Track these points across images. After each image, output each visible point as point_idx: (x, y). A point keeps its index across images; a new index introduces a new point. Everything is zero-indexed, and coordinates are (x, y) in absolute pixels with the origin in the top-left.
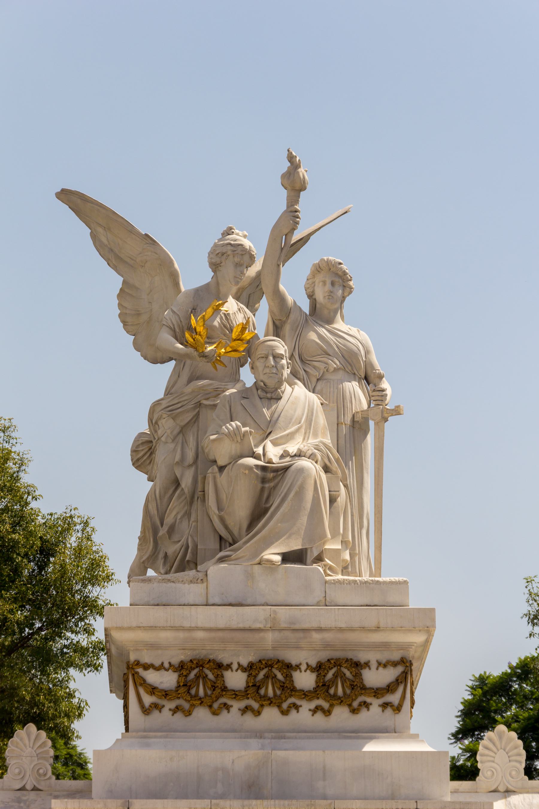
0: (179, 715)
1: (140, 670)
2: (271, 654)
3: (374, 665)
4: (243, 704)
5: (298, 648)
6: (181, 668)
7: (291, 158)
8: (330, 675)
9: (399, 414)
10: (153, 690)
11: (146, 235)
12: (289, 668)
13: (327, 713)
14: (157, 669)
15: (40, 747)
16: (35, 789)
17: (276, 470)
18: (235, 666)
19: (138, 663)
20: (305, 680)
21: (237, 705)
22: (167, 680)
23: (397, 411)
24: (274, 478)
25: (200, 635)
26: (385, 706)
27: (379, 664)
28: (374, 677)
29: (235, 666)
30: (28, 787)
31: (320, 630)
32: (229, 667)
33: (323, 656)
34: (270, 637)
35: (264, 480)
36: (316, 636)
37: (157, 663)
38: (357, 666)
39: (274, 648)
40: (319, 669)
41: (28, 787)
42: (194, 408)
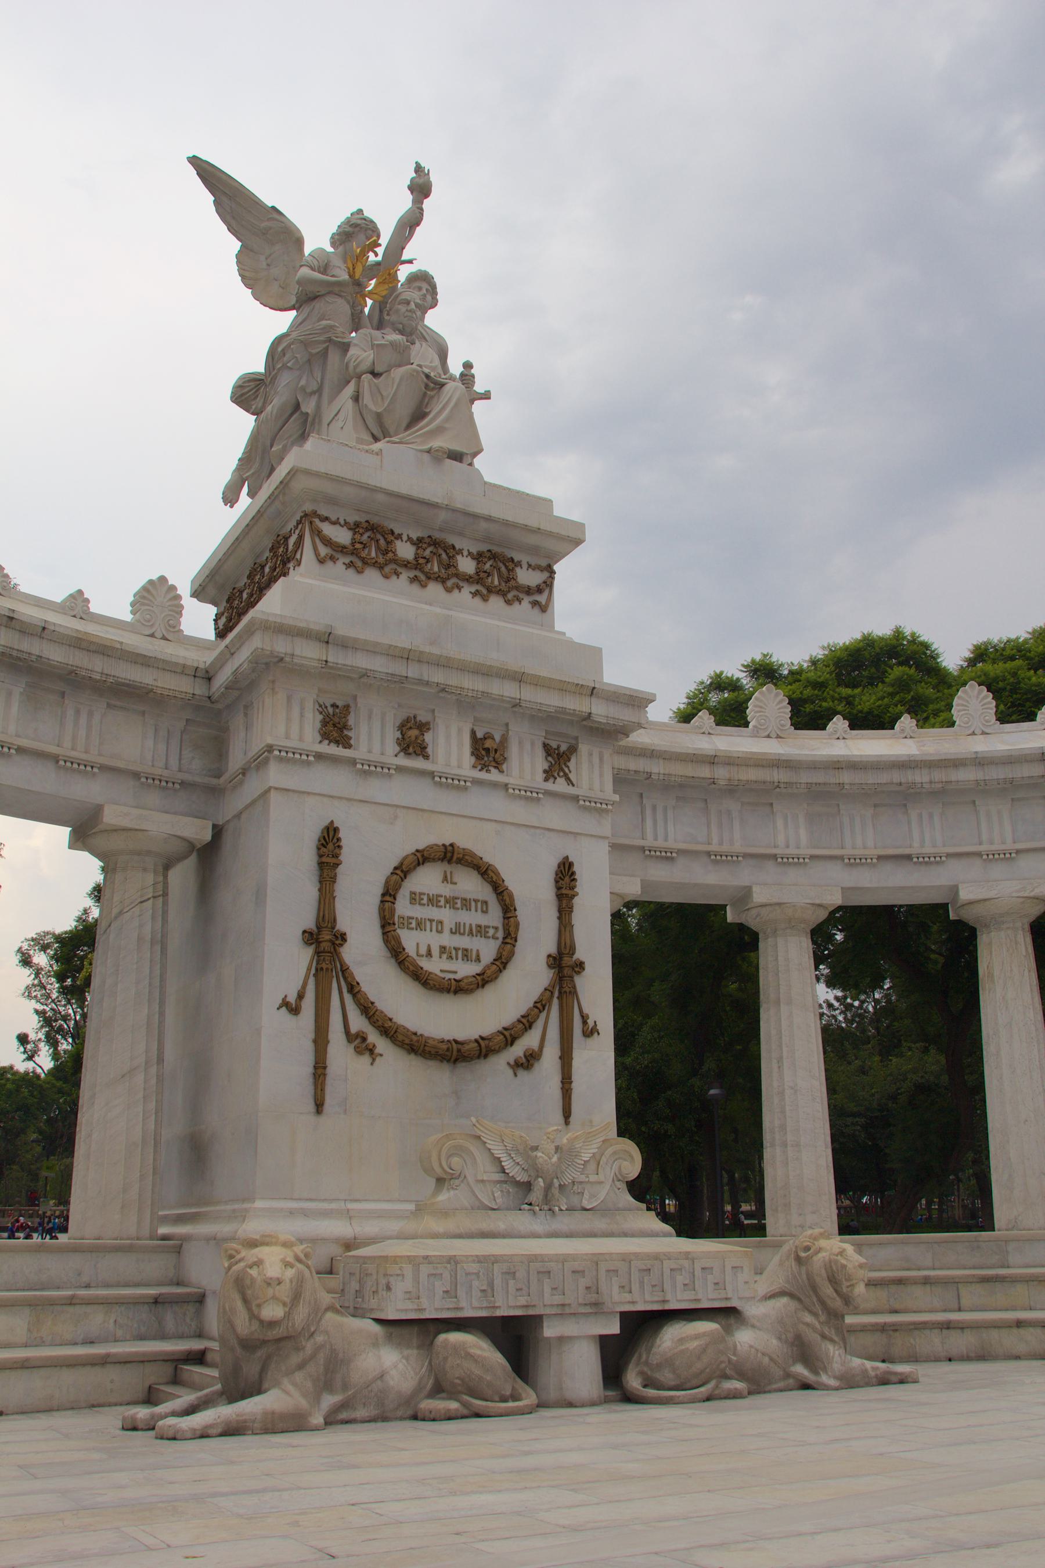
0: (351, 571)
1: (317, 521)
2: (437, 535)
3: (525, 566)
4: (412, 574)
5: (461, 534)
6: (355, 527)
7: (419, 169)
8: (487, 566)
9: (489, 398)
10: (328, 542)
11: (273, 208)
12: (452, 551)
13: (485, 599)
14: (334, 523)
15: (170, 599)
16: (164, 638)
17: (436, 383)
18: (405, 538)
19: (315, 514)
20: (466, 565)
21: (405, 575)
22: (343, 536)
23: (486, 396)
24: (433, 389)
25: (381, 497)
26: (535, 603)
27: (529, 566)
28: (526, 577)
29: (405, 538)
30: (158, 635)
31: (489, 519)
32: (399, 537)
33: (484, 547)
34: (443, 516)
35: (427, 386)
36: (484, 525)
37: (334, 519)
38: (512, 564)
39: (441, 530)
40: (478, 557)
41: (158, 635)
42: (325, 342)
